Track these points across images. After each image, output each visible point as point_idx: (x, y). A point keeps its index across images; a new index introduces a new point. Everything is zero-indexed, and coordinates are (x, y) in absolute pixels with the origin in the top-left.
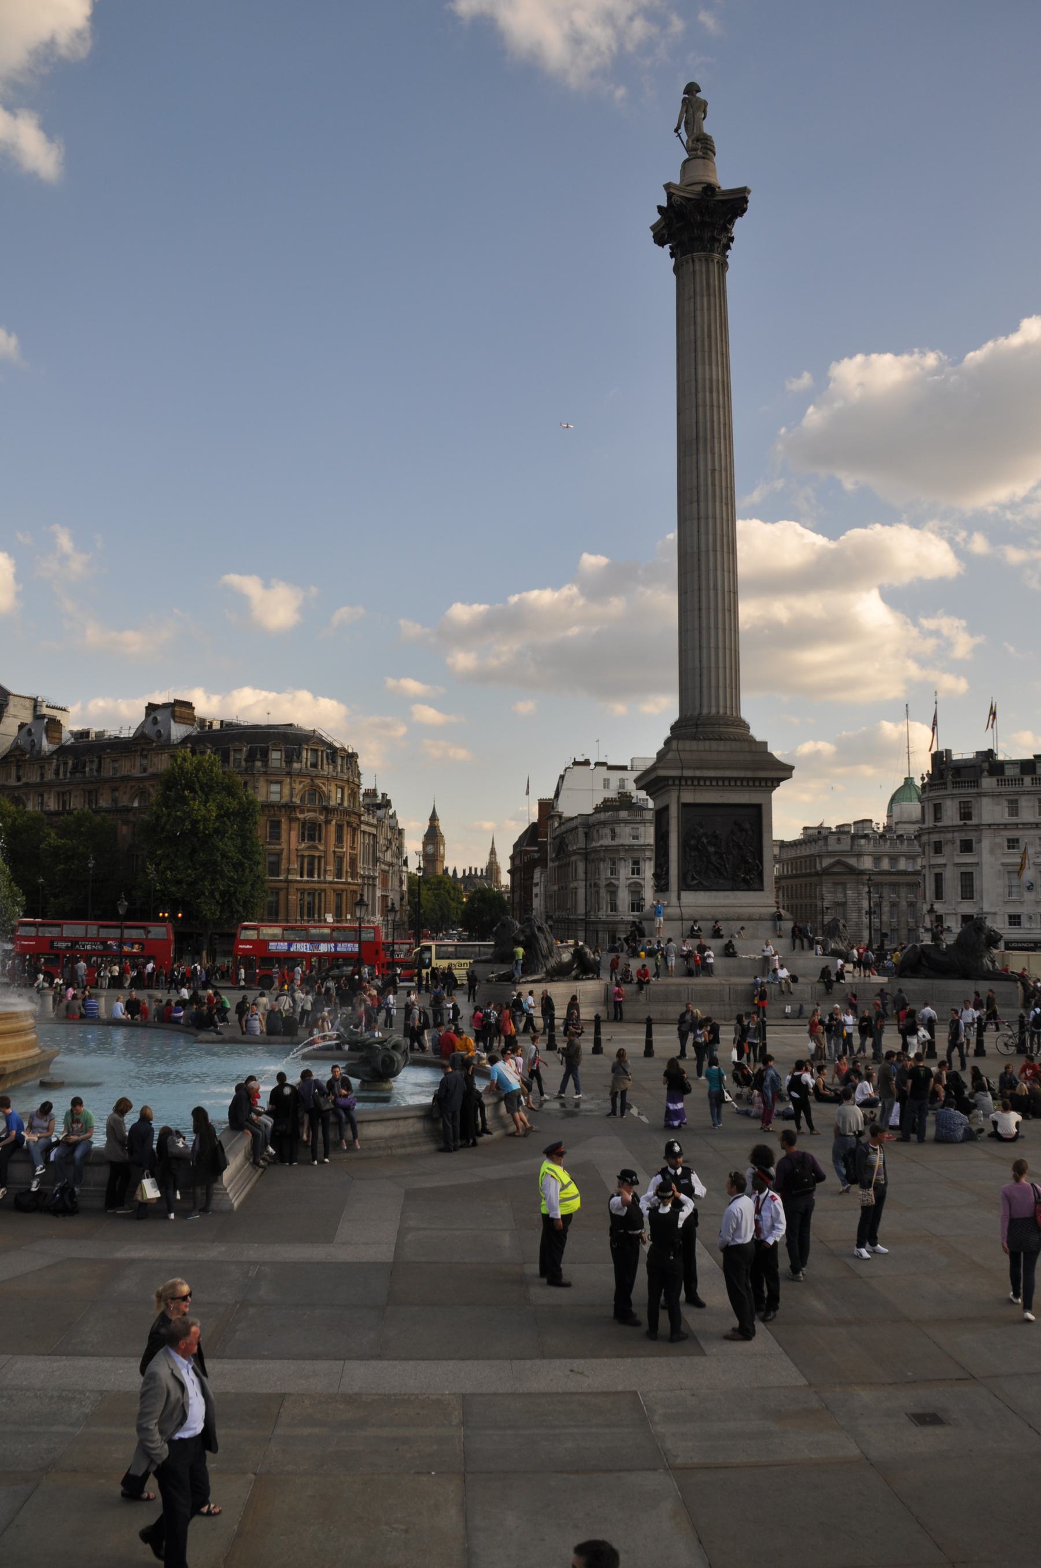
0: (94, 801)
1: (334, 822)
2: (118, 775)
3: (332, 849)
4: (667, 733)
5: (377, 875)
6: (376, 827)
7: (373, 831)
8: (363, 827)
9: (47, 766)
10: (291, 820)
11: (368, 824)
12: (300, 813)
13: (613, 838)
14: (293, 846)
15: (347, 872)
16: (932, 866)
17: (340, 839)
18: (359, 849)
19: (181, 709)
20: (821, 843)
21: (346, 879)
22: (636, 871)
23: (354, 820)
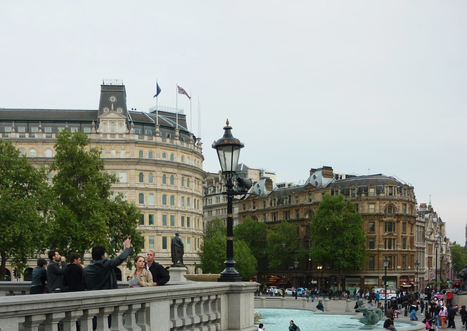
0: (288, 216)
1: (401, 222)
2: (299, 204)
3: (401, 235)
5: (425, 247)
6: (424, 223)
7: (423, 225)
8: (417, 223)
9: (267, 201)
10: (380, 221)
11: (419, 222)
12: (384, 218)
14: (381, 234)
15: (408, 246)
17: (404, 229)
18: (415, 234)
19: (327, 171)
21: (408, 249)
23: (412, 220)
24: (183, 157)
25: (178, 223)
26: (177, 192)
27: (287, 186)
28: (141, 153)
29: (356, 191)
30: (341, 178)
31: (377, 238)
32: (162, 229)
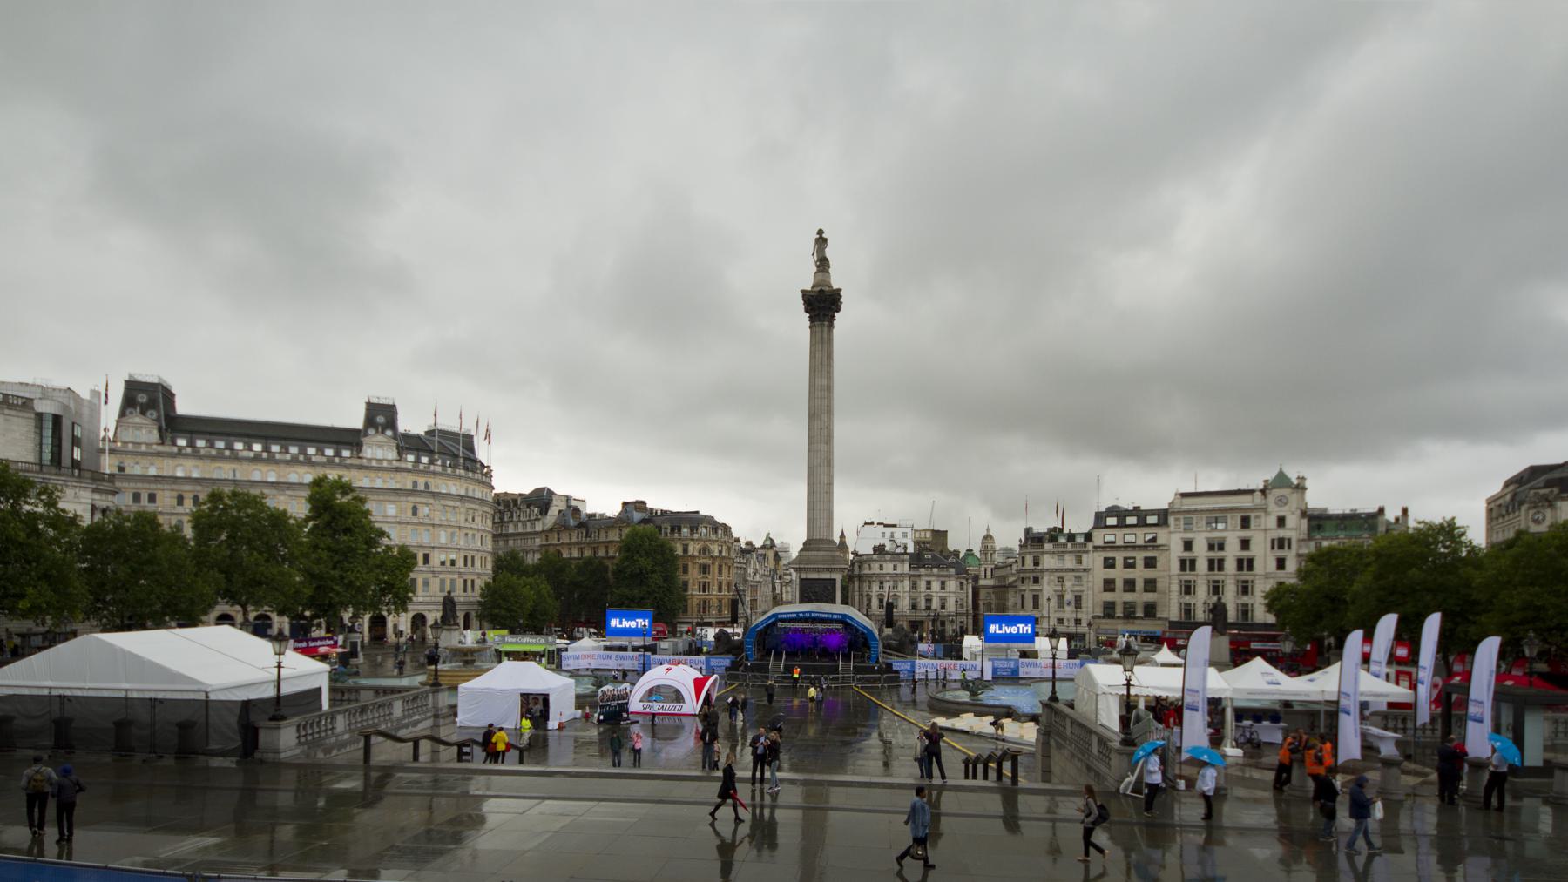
4: (802, 546)
6: (745, 564)
8: (735, 565)
10: (693, 563)
11: (739, 563)
13: (870, 569)
16: (1021, 591)
17: (720, 572)
19: (640, 505)
20: (1009, 568)
22: (881, 587)
23: (730, 562)
24: (467, 489)
25: (460, 563)
26: (460, 527)
27: (597, 517)
28: (415, 483)
29: (669, 531)
30: (656, 513)
31: (691, 581)
32: (440, 570)
